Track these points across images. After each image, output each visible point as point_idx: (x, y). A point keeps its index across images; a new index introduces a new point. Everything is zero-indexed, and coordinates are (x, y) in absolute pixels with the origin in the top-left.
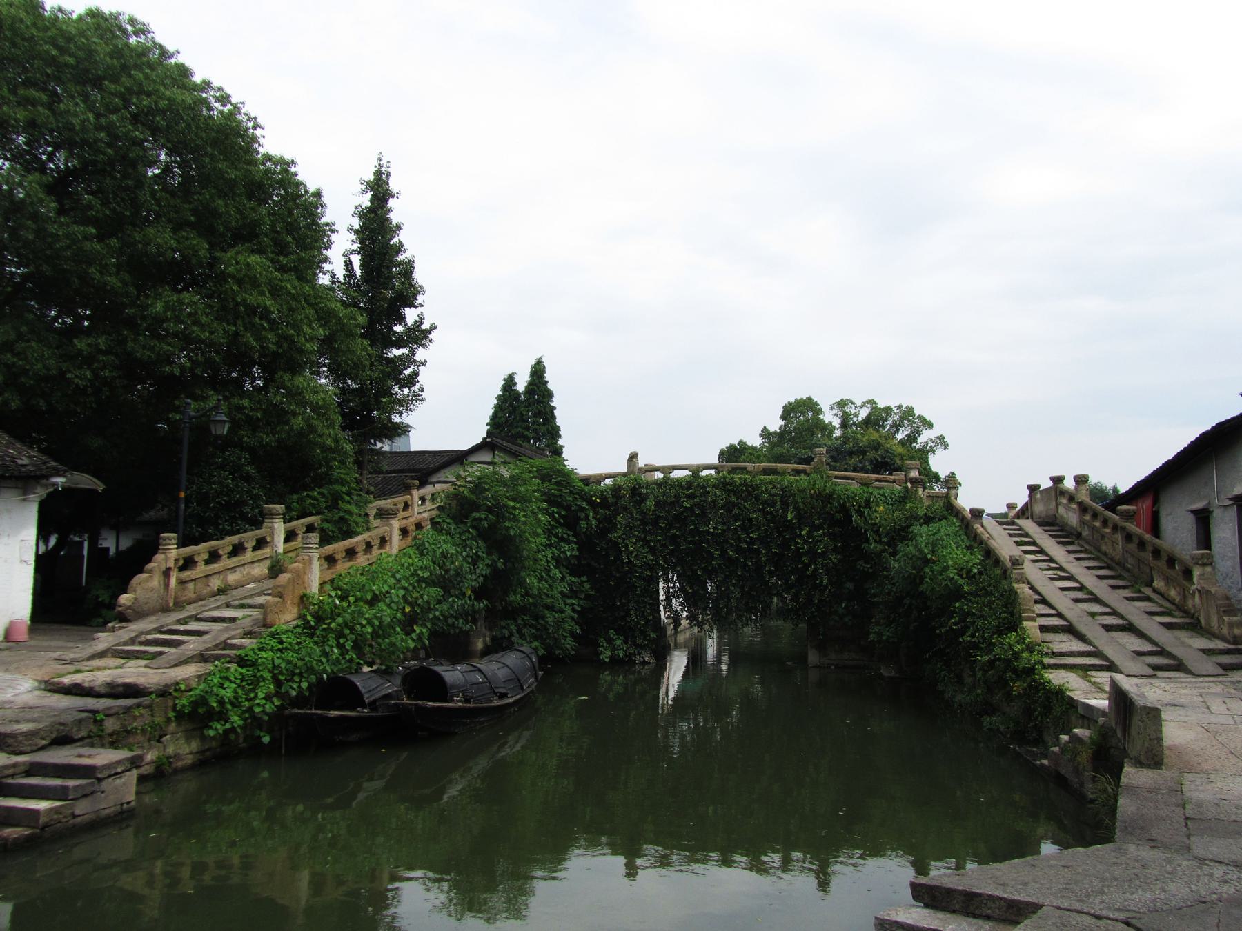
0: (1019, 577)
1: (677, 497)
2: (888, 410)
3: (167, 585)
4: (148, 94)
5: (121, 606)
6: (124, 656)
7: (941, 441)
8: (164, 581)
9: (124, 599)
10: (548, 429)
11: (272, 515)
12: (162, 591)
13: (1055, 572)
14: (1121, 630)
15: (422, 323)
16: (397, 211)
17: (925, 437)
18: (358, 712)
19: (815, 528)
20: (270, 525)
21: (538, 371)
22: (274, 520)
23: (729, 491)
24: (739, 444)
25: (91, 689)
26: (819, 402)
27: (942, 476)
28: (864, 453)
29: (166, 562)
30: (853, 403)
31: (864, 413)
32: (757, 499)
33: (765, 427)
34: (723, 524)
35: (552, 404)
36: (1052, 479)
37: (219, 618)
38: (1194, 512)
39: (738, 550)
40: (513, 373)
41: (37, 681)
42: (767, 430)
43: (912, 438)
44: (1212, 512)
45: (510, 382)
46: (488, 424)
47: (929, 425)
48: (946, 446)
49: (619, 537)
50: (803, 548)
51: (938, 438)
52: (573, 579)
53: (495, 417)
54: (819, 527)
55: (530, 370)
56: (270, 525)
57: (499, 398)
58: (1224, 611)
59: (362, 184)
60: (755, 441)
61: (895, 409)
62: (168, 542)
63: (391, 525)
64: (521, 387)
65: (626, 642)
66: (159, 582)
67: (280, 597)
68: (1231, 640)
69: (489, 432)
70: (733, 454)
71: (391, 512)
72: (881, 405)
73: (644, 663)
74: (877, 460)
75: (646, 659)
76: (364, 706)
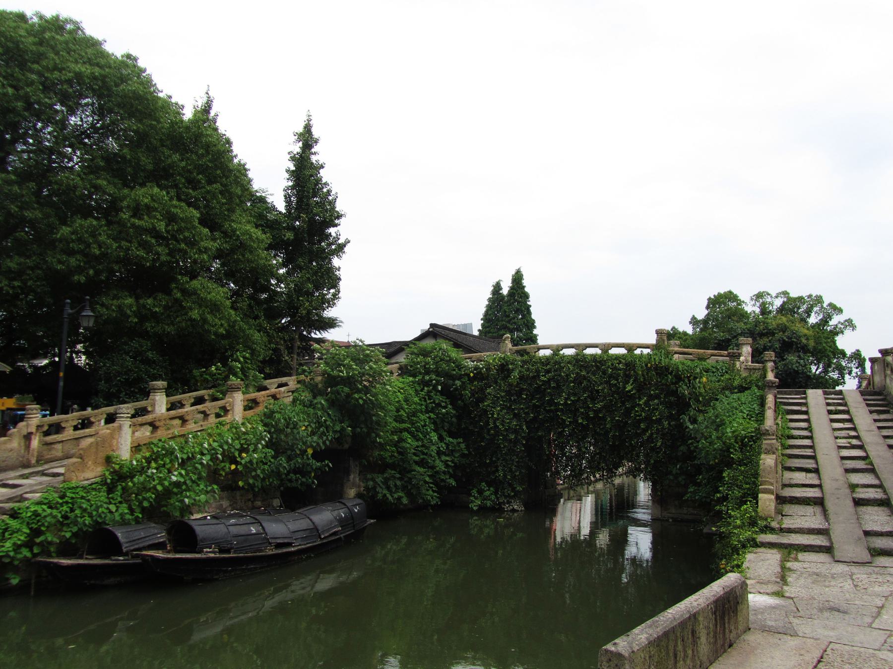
0: (769, 448)
1: (538, 371)
2: (800, 299)
3: (28, 446)
4: (60, 70)
7: (850, 324)
8: (25, 442)
10: (524, 322)
11: (155, 390)
12: (23, 451)
13: (848, 440)
14: (879, 505)
15: (339, 239)
16: (320, 154)
17: (835, 320)
18: (112, 560)
19: (651, 398)
21: (518, 279)
22: (156, 394)
23: (582, 366)
24: (672, 330)
26: (738, 295)
27: (848, 353)
28: (773, 334)
29: (27, 428)
30: (769, 294)
31: (778, 303)
32: (604, 372)
33: (694, 316)
34: (575, 394)
35: (528, 303)
36: (881, 351)
39: (587, 417)
42: (695, 318)
43: (825, 321)
45: (497, 287)
46: (482, 319)
47: (840, 311)
48: (854, 327)
49: (488, 405)
50: (641, 415)
51: (846, 321)
52: (451, 440)
53: (486, 314)
54: (657, 397)
55: (511, 278)
57: (489, 300)
59: (295, 135)
61: (806, 298)
63: (234, 397)
64: (505, 291)
65: (496, 493)
66: (19, 444)
67: (81, 458)
69: (483, 325)
70: (667, 336)
71: (234, 386)
72: (794, 294)
73: (514, 511)
74: (784, 340)
75: (515, 507)
76: (121, 553)
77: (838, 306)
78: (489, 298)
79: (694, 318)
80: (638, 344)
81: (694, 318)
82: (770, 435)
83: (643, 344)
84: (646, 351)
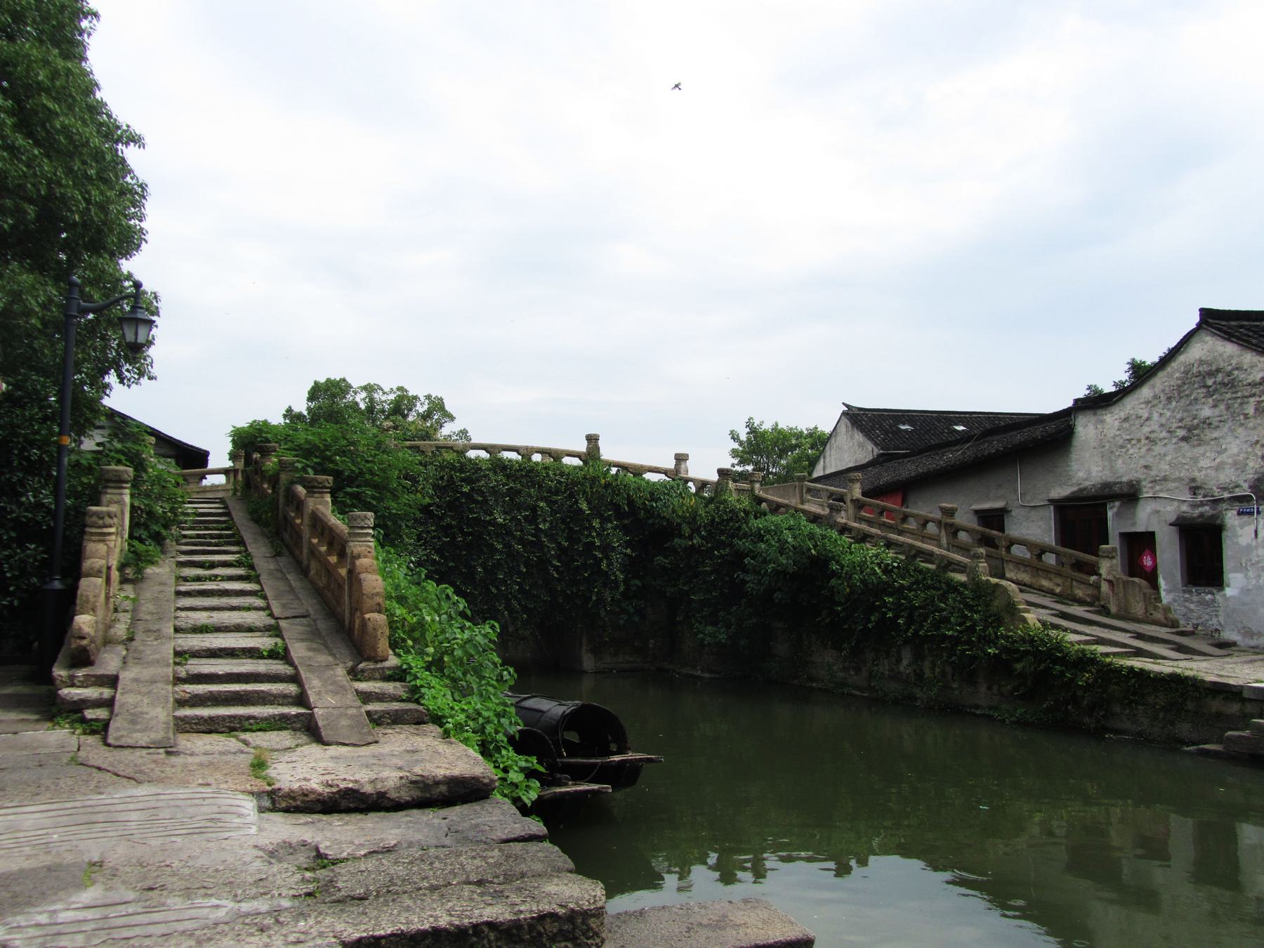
5: (84, 638)
6: (203, 728)
9: (84, 621)
19: (604, 520)
20: (116, 498)
25: (382, 795)
33: (290, 407)
37: (221, 650)
39: (521, 541)
41: (252, 793)
44: (1011, 511)
47: (452, 418)
51: (461, 431)
54: (608, 520)
56: (116, 498)
60: (277, 419)
61: (422, 399)
62: (108, 521)
68: (1170, 624)
79: (289, 410)
80: (568, 451)
81: (289, 410)
83: (573, 452)
84: (576, 462)
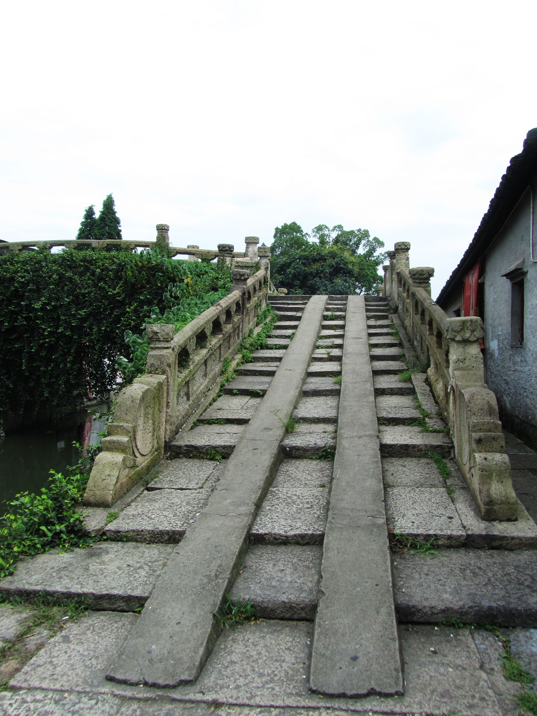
0: (157, 363)
2: (352, 232)
21: (109, 204)
26: (301, 226)
28: (325, 260)
30: (327, 228)
32: (93, 274)
35: (119, 228)
38: (507, 275)
40: (92, 206)
42: (265, 246)
43: (370, 253)
45: (90, 213)
57: (83, 224)
58: (479, 441)
61: (356, 232)
64: (97, 215)
72: (347, 229)
77: (381, 240)
78: (83, 223)
82: (159, 341)
